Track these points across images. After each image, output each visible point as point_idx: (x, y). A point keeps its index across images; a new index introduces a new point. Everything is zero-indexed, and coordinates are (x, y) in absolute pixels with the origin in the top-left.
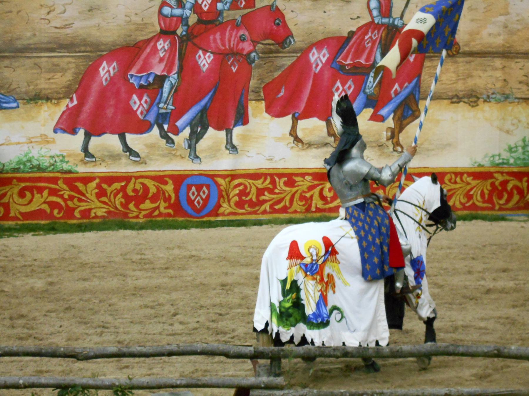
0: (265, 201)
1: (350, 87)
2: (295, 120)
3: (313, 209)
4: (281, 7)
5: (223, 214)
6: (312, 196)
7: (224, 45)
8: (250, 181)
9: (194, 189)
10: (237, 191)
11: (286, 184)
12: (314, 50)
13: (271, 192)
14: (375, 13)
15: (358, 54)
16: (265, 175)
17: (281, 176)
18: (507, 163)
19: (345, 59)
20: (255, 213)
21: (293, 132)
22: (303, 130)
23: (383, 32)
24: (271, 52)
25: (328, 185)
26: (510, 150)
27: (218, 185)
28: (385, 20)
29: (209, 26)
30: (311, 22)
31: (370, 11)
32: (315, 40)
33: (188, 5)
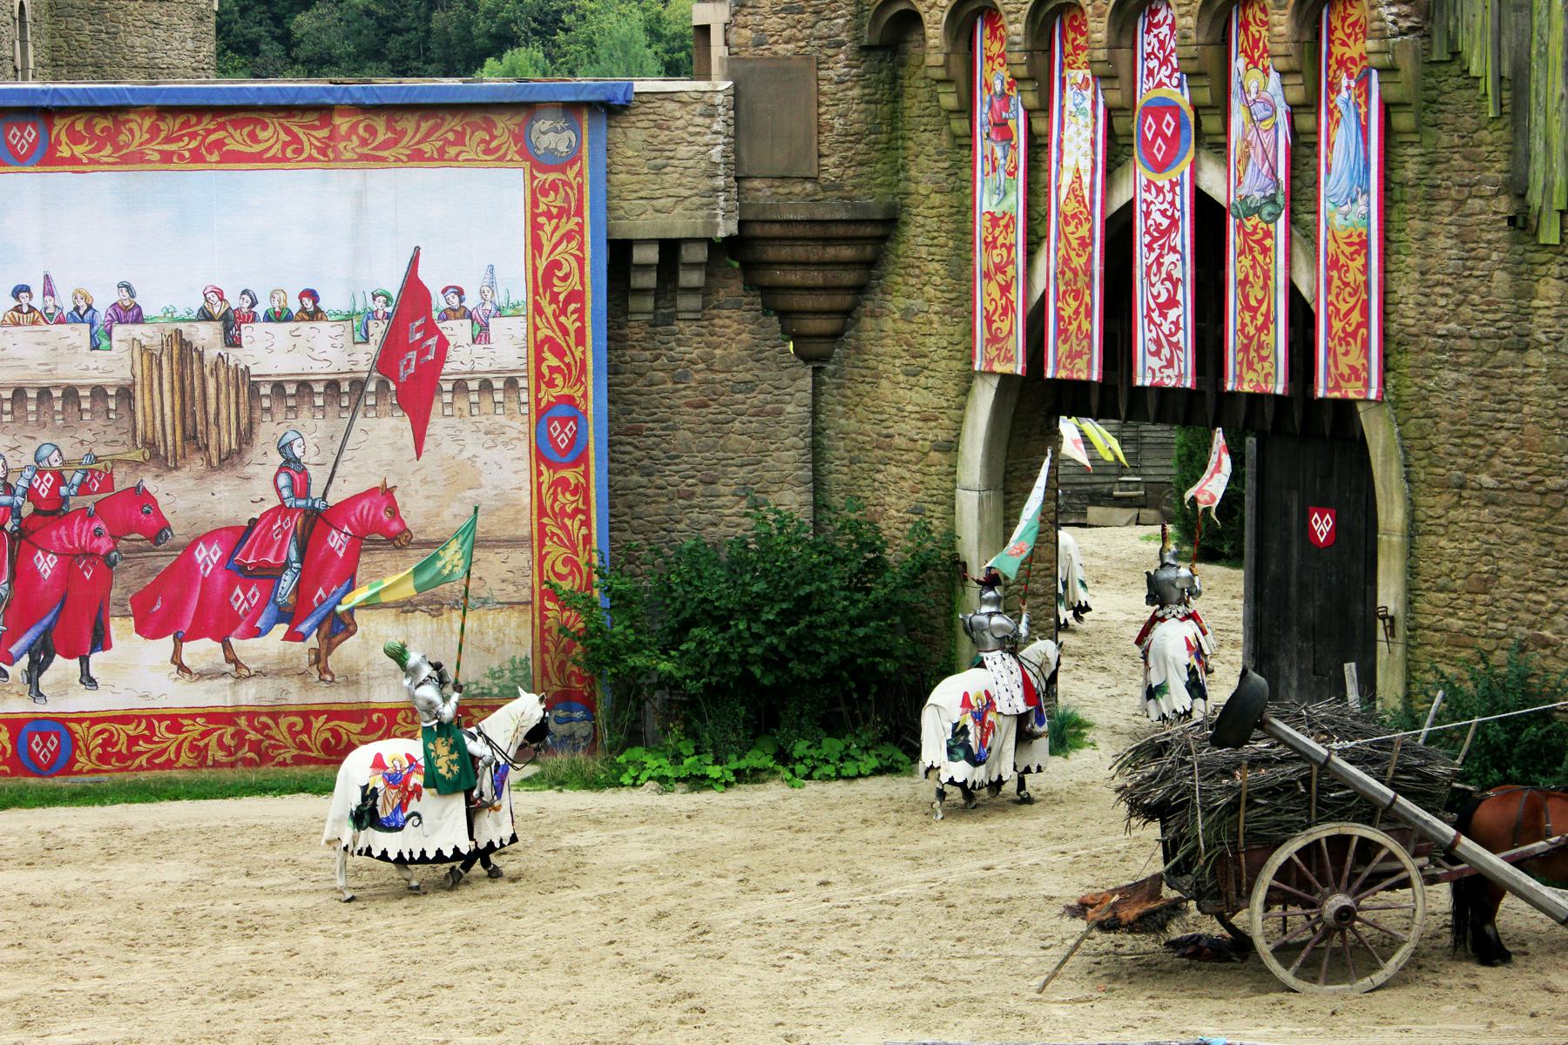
0: (140, 754)
1: (254, 595)
2: (179, 641)
3: (210, 762)
4: (151, 490)
5: (80, 772)
6: (207, 745)
7: (72, 543)
8: (118, 726)
9: (37, 738)
10: (99, 740)
11: (168, 729)
12: (201, 546)
13: (148, 740)
14: (286, 493)
15: (264, 549)
16: (139, 718)
17: (161, 718)
18: (490, 694)
19: (246, 556)
20: (126, 769)
21: (176, 659)
22: (190, 655)
23: (298, 520)
24: (140, 550)
25: (230, 730)
26: (493, 675)
27: (71, 733)
28: (301, 503)
29: (49, 519)
30: (193, 508)
31: (279, 491)
32: (201, 532)
33: (20, 491)
